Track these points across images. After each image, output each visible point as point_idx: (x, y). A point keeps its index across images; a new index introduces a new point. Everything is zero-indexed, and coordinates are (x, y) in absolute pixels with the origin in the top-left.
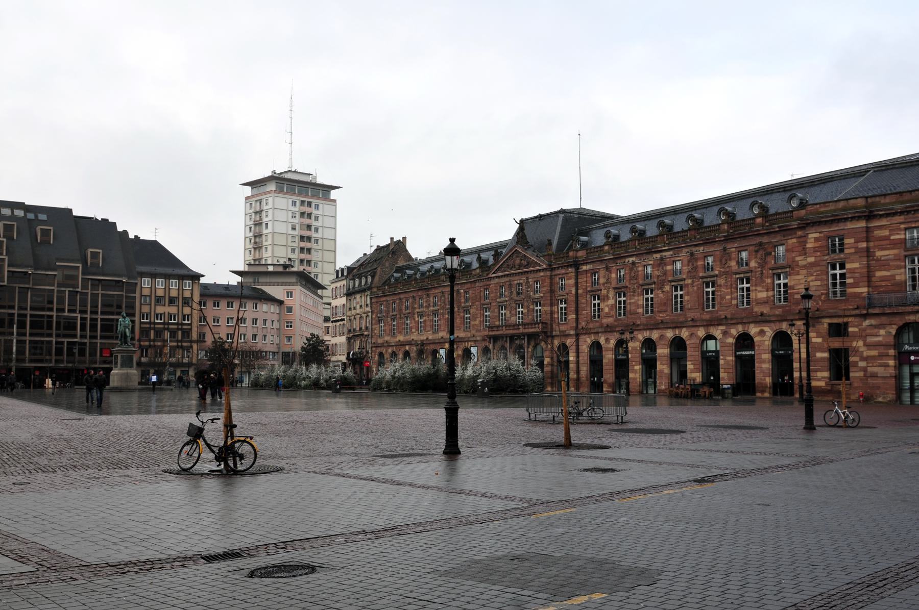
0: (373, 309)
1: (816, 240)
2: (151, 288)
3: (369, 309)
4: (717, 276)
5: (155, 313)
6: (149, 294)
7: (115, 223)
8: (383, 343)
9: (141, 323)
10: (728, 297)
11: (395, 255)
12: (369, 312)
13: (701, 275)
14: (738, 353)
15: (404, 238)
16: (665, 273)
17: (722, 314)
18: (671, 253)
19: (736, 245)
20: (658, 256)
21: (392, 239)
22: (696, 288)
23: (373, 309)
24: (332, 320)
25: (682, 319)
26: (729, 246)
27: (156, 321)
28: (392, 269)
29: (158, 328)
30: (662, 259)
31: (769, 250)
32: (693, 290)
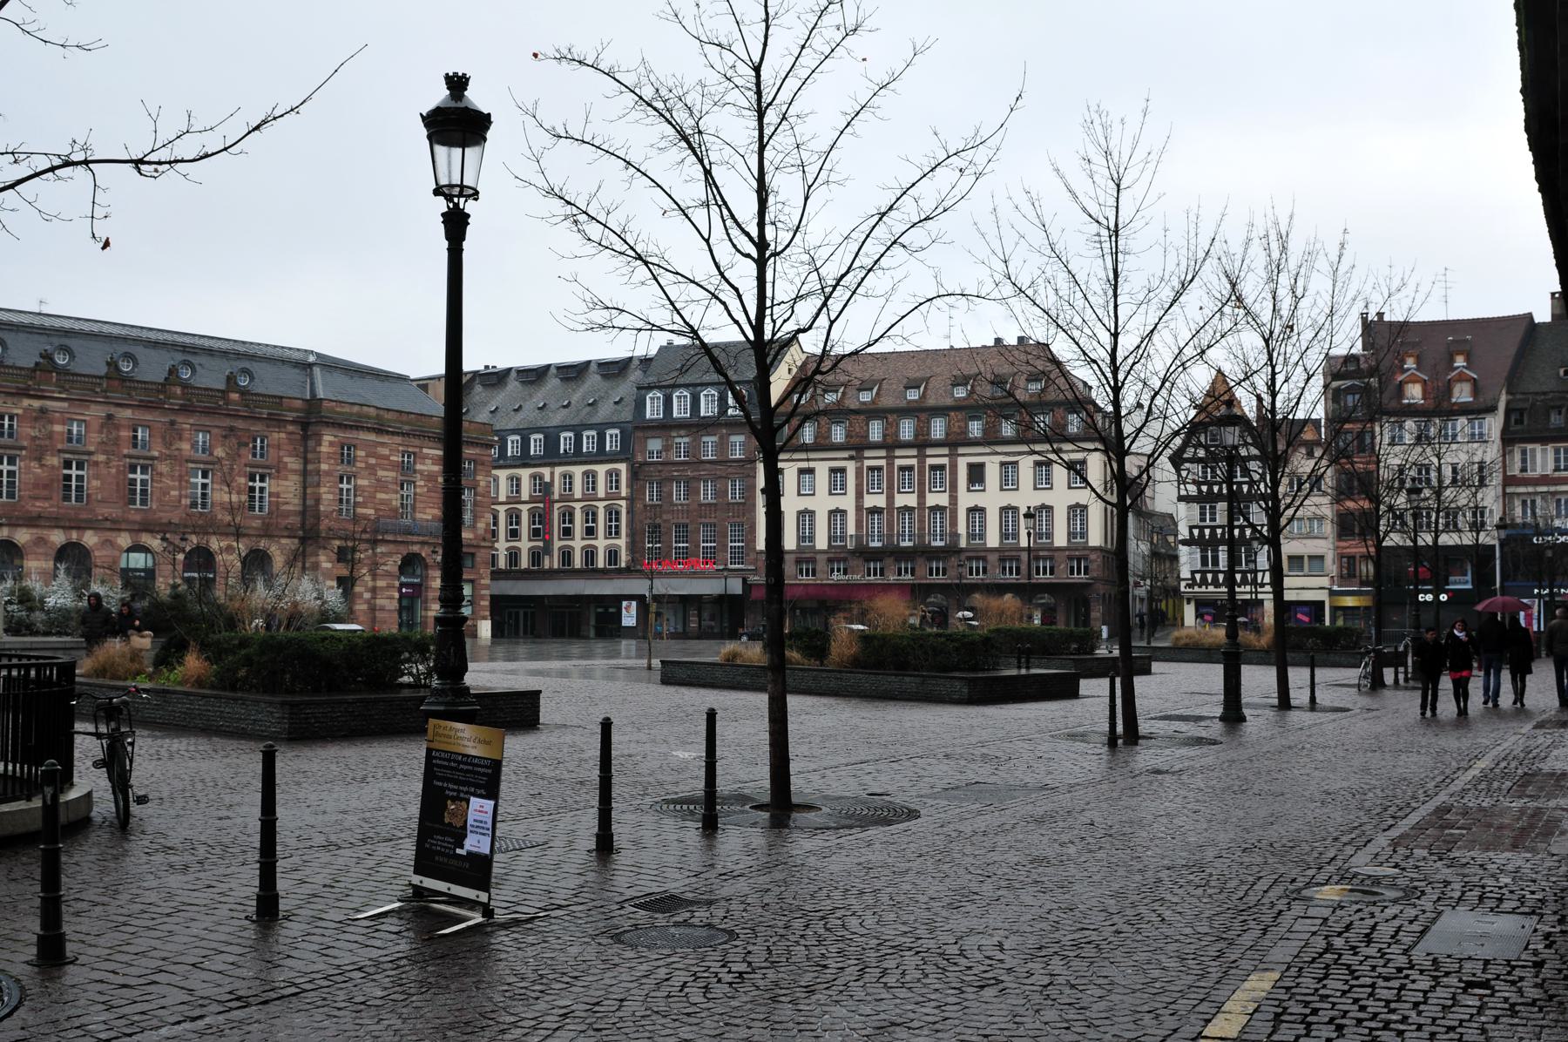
1: (331, 444)
4: (153, 458)
10: (174, 493)
13: (125, 451)
14: (186, 575)
16: (50, 436)
17: (165, 517)
18: (65, 405)
19: (191, 421)
20: (36, 404)
22: (113, 471)
25: (84, 516)
26: (180, 419)
30: (43, 411)
31: (245, 440)
32: (109, 473)
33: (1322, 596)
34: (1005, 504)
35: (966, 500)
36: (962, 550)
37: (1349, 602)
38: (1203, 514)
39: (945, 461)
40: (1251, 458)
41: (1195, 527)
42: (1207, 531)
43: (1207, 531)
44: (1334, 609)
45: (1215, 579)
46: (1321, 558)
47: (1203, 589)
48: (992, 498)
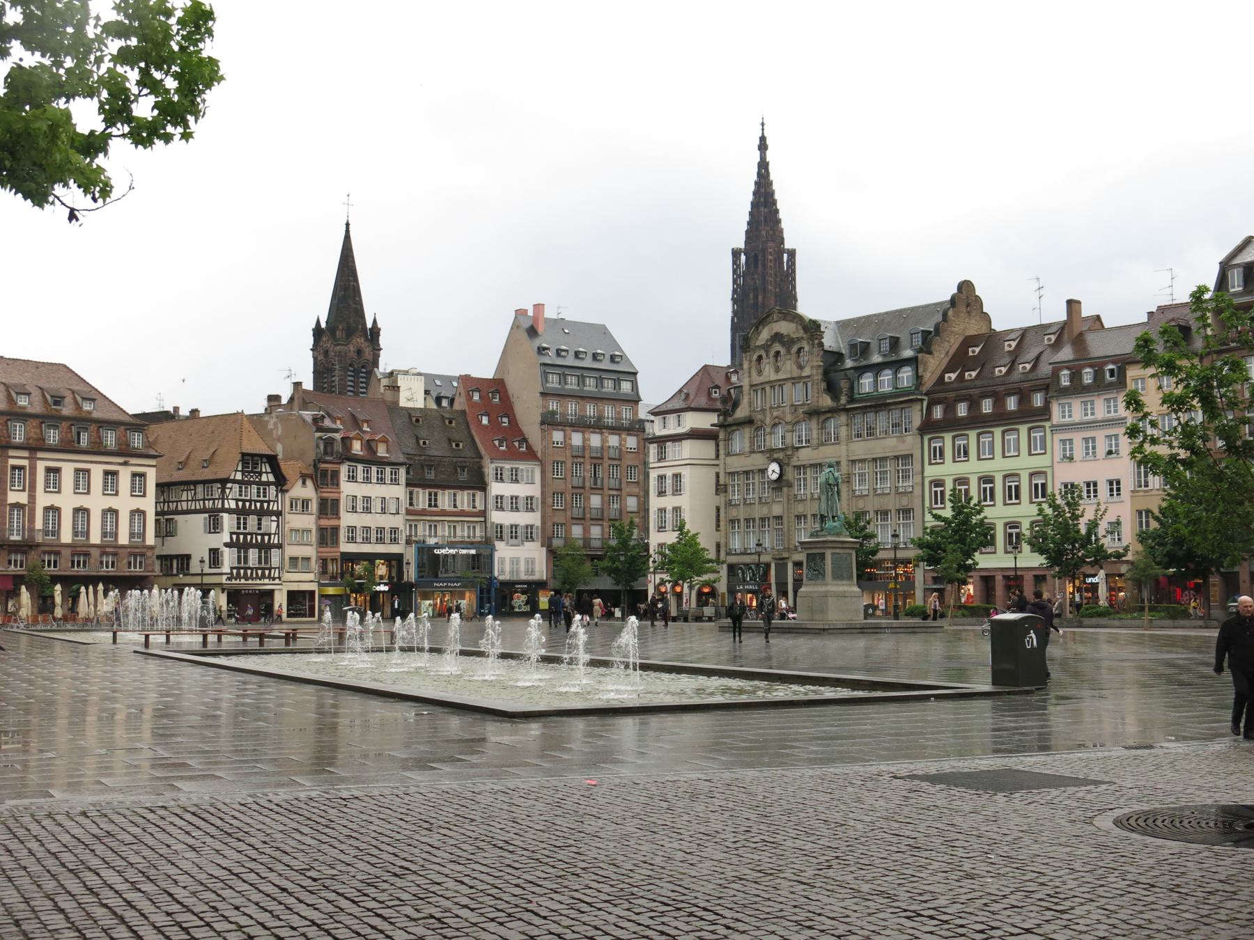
33: (313, 587)
34: (78, 506)
35: (43, 500)
36: (38, 545)
37: (331, 591)
38: (239, 523)
39: (25, 463)
40: (268, 484)
41: (234, 533)
42: (241, 537)
43: (241, 537)
44: (322, 596)
45: (245, 573)
46: (308, 559)
47: (238, 582)
48: (67, 501)
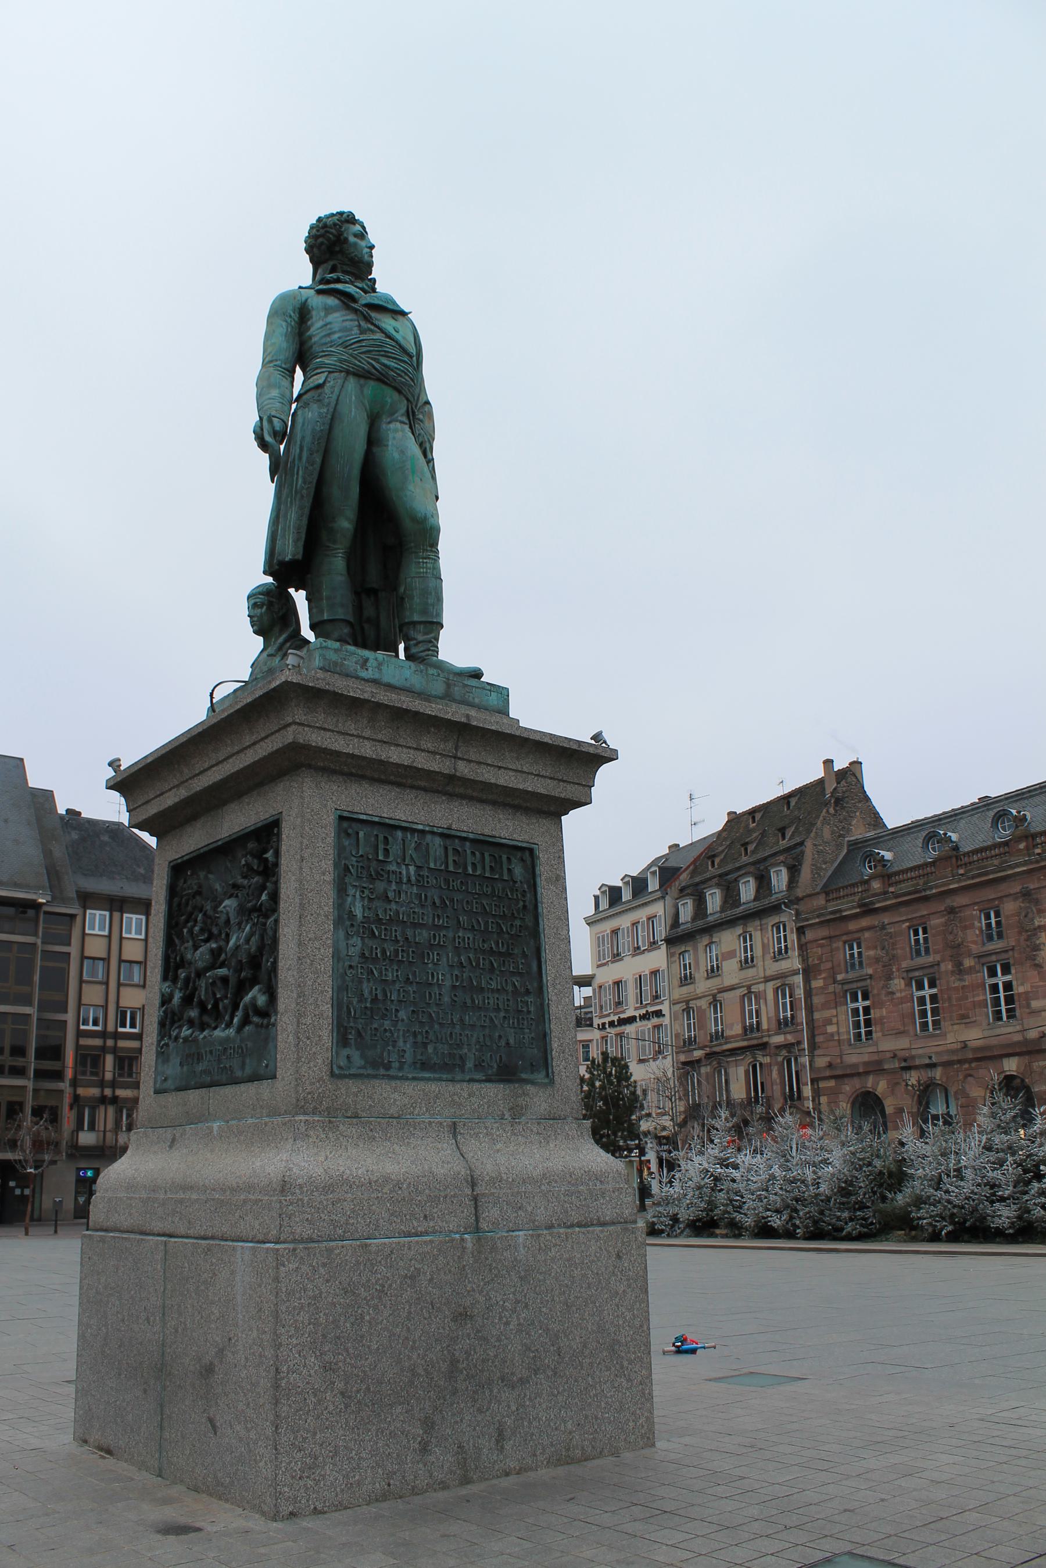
0: (813, 961)
2: (109, 936)
3: (794, 962)
5: (118, 1006)
6: (104, 955)
7: (22, 760)
8: (879, 1062)
9: (80, 1034)
11: (843, 808)
12: (795, 973)
15: (857, 764)
21: (828, 763)
23: (813, 961)
24: (597, 1022)
27: (121, 1030)
28: (839, 846)
29: (123, 1049)
